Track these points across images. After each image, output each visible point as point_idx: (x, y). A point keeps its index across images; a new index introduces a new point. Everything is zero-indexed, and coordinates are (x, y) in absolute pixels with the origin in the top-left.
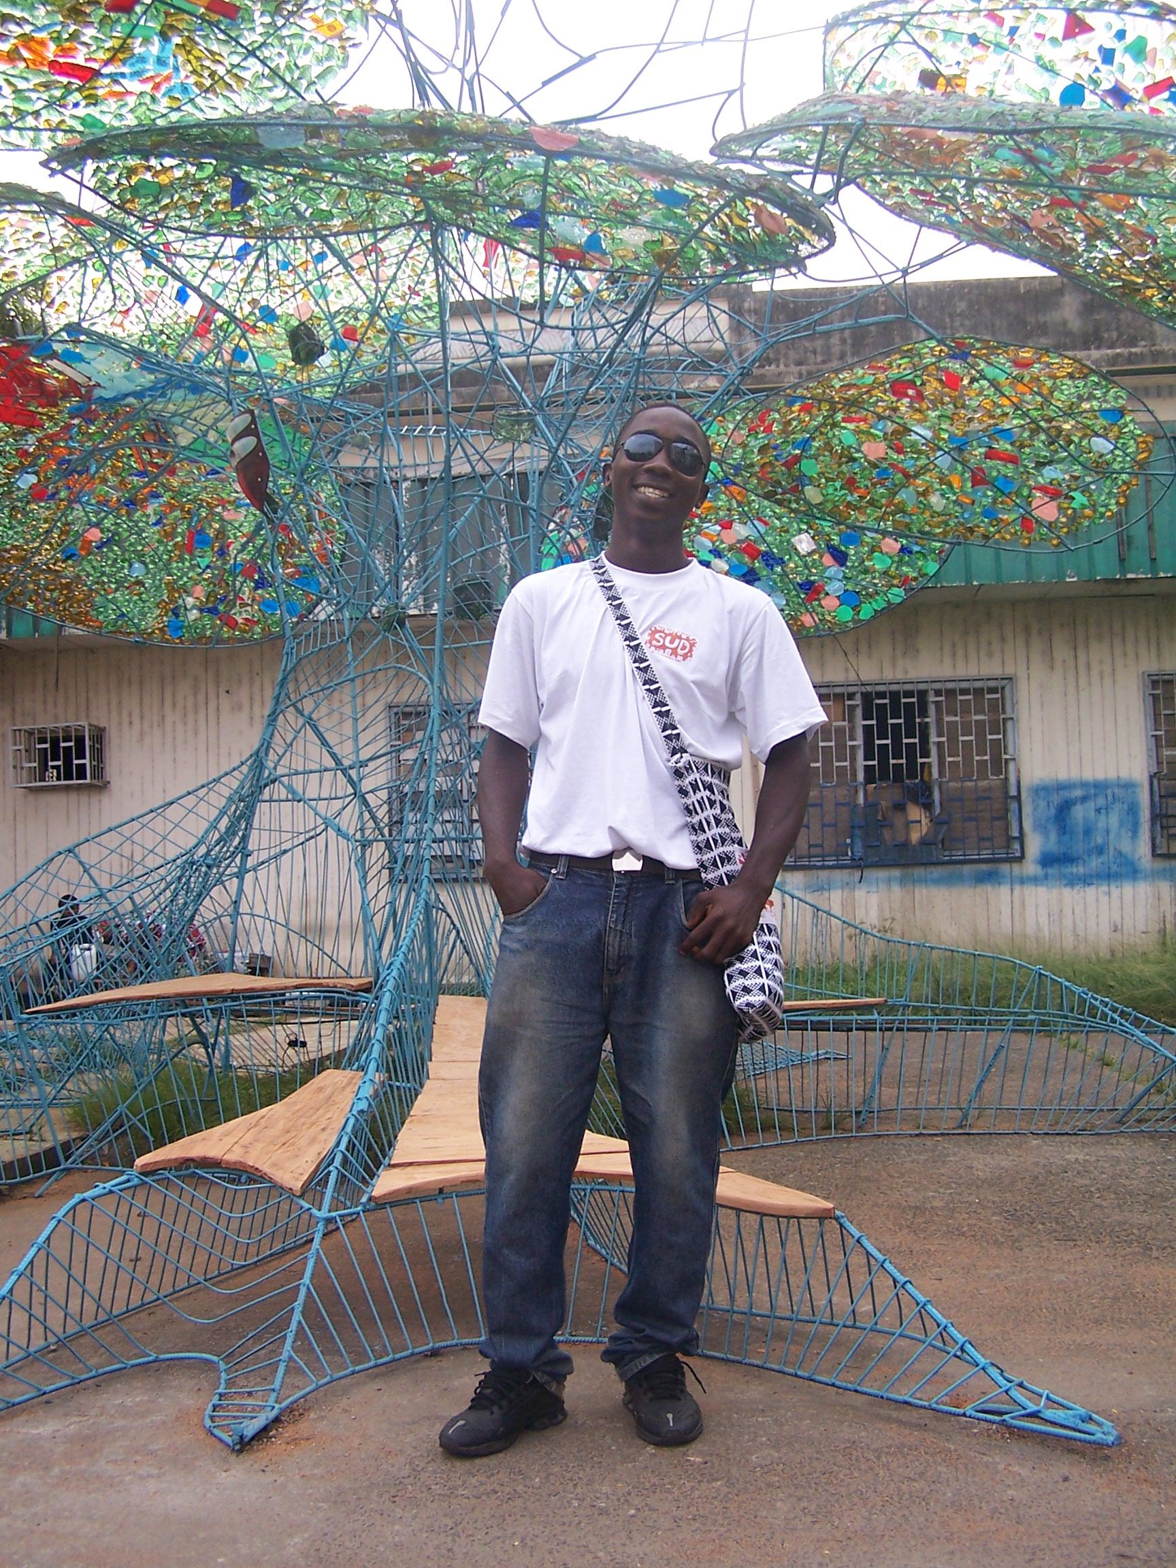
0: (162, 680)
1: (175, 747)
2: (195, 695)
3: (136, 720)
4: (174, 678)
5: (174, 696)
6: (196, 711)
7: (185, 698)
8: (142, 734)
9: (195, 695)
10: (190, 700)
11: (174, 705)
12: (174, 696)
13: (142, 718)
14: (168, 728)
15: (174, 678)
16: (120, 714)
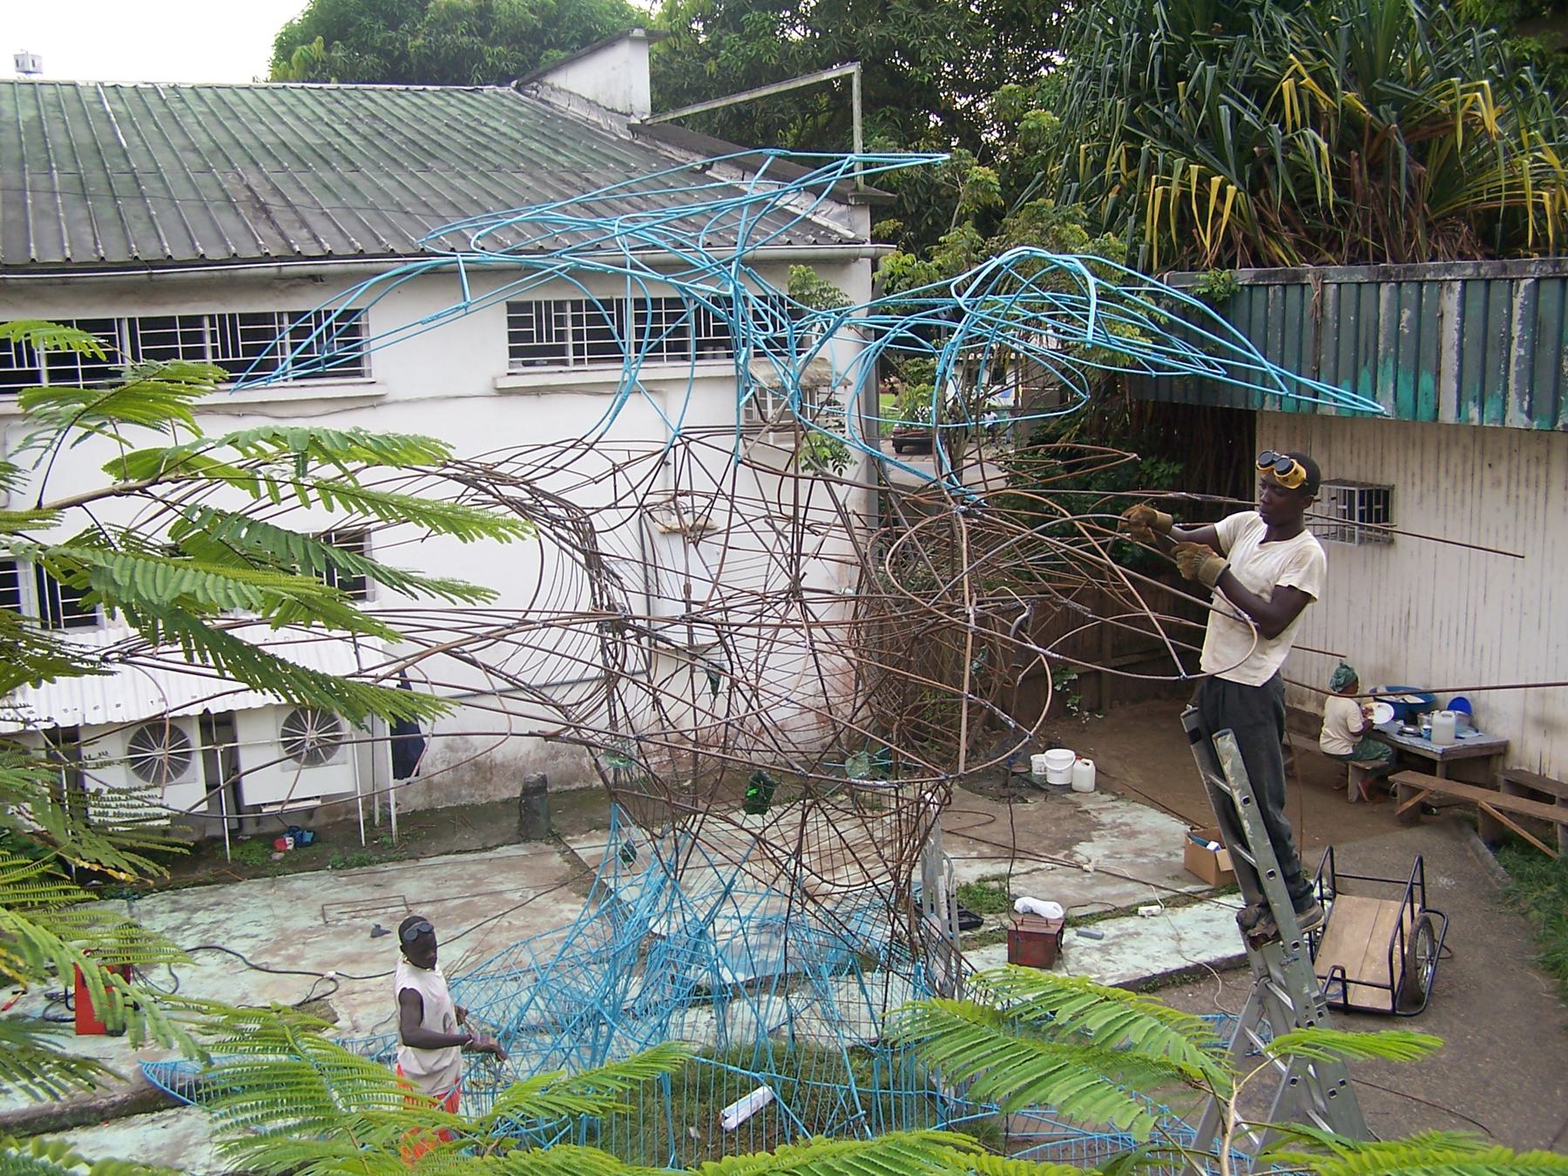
0: (1439, 443)
1: (1445, 512)
2: (1465, 462)
3: (1417, 481)
4: (1448, 445)
5: (1447, 461)
6: (1464, 481)
7: (1456, 466)
8: (1421, 496)
9: (1465, 462)
10: (1460, 468)
11: (1447, 472)
12: (1447, 461)
13: (1422, 480)
14: (1442, 495)
15: (1448, 445)
16: (1406, 474)
